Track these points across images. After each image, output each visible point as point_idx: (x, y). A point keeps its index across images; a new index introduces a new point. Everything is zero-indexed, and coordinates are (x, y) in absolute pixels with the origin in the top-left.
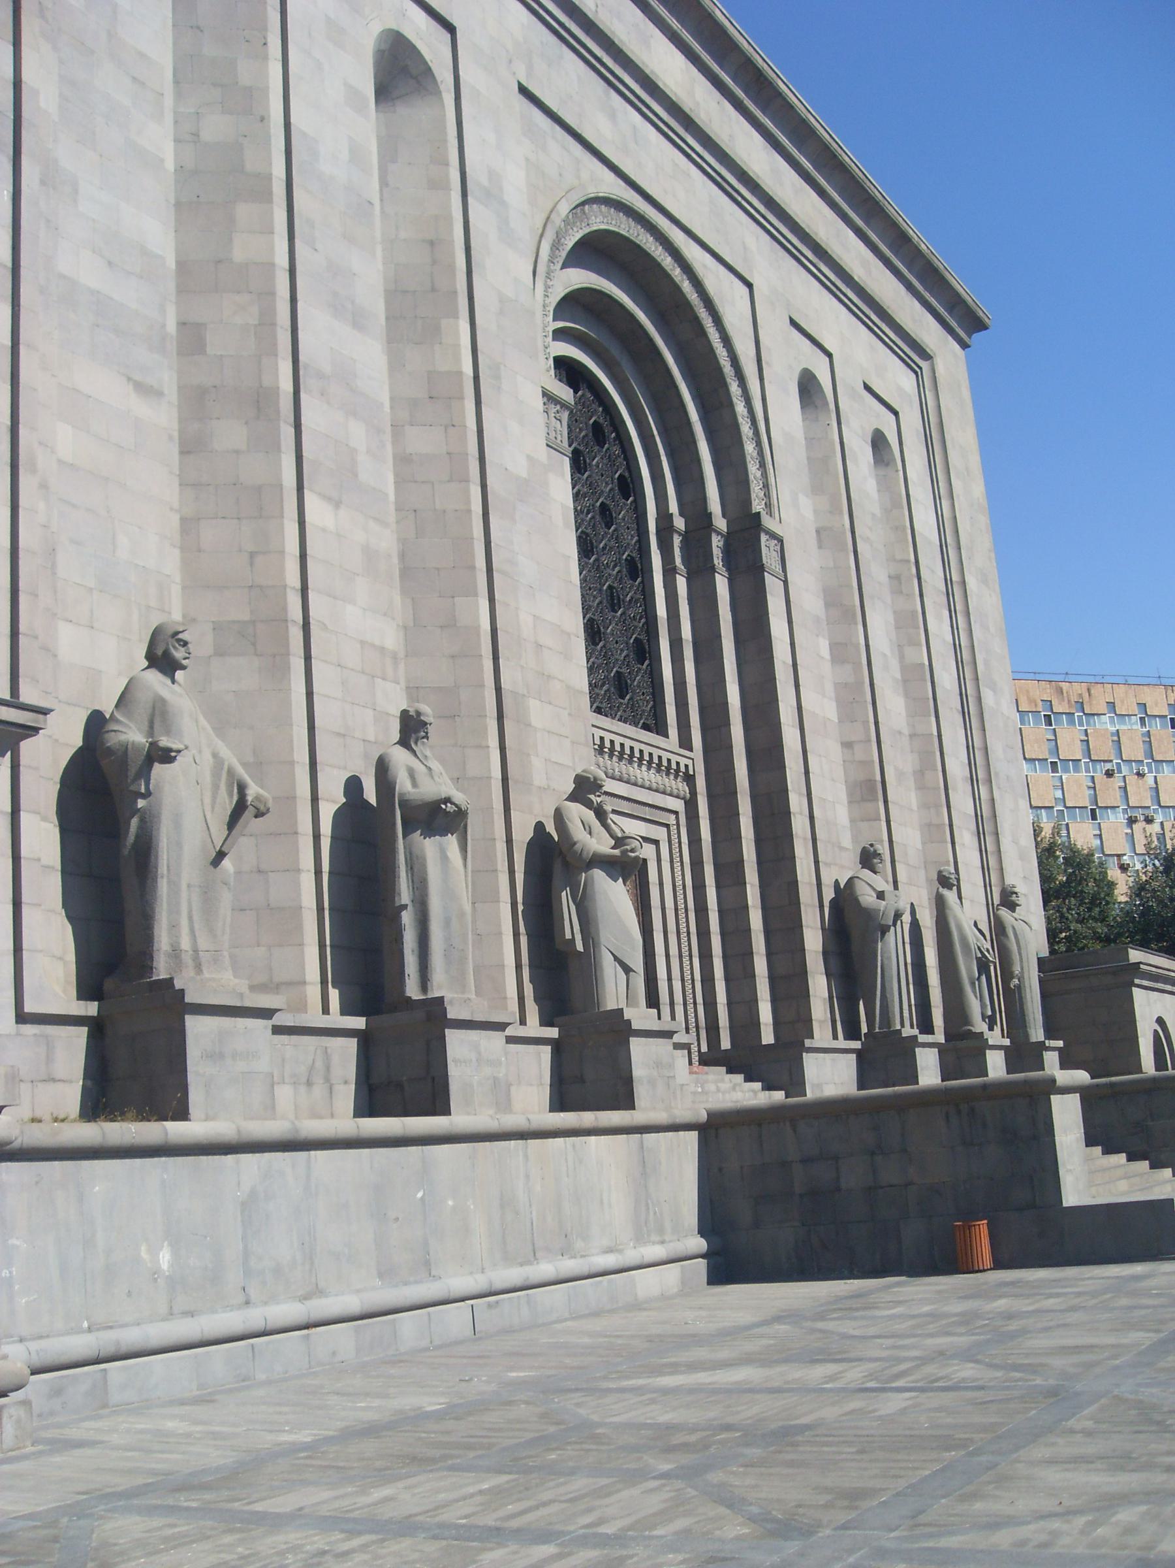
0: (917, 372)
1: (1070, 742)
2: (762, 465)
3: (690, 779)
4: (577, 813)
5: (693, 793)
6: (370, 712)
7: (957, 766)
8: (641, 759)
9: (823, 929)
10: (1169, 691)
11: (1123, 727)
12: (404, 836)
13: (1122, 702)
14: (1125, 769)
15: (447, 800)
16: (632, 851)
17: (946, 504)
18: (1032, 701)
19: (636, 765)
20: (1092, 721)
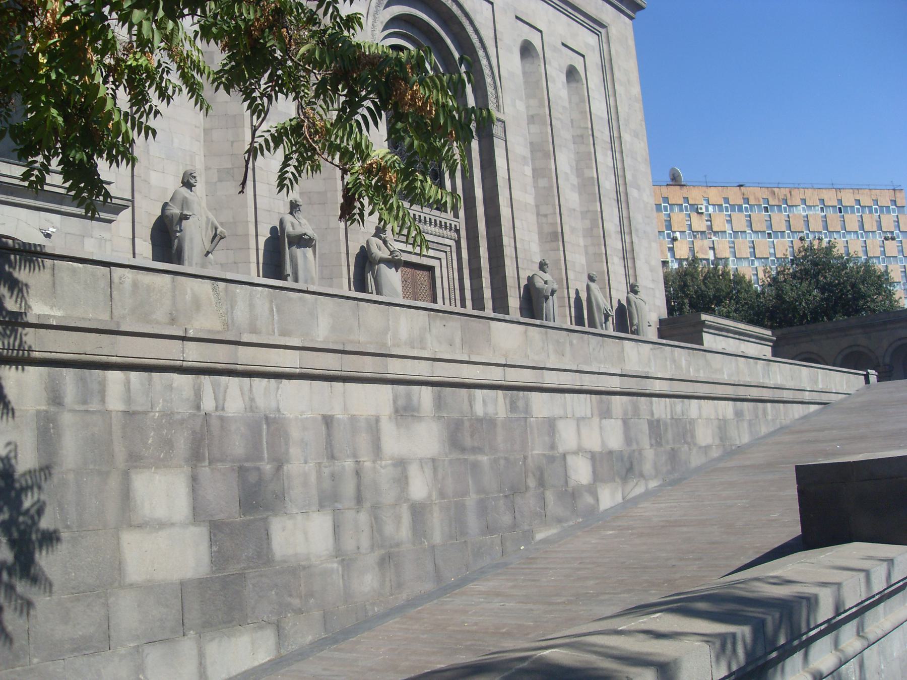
0: (598, 34)
1: (779, 221)
2: (495, 88)
3: (457, 231)
4: (375, 241)
5: (459, 237)
6: (282, 202)
7: (612, 225)
8: (431, 223)
9: (520, 298)
10: (838, 192)
11: (810, 213)
12: (289, 248)
13: (810, 199)
14: (811, 237)
15: (305, 234)
16: (396, 256)
17: (612, 99)
18: (757, 199)
19: (428, 225)
20: (792, 209)
